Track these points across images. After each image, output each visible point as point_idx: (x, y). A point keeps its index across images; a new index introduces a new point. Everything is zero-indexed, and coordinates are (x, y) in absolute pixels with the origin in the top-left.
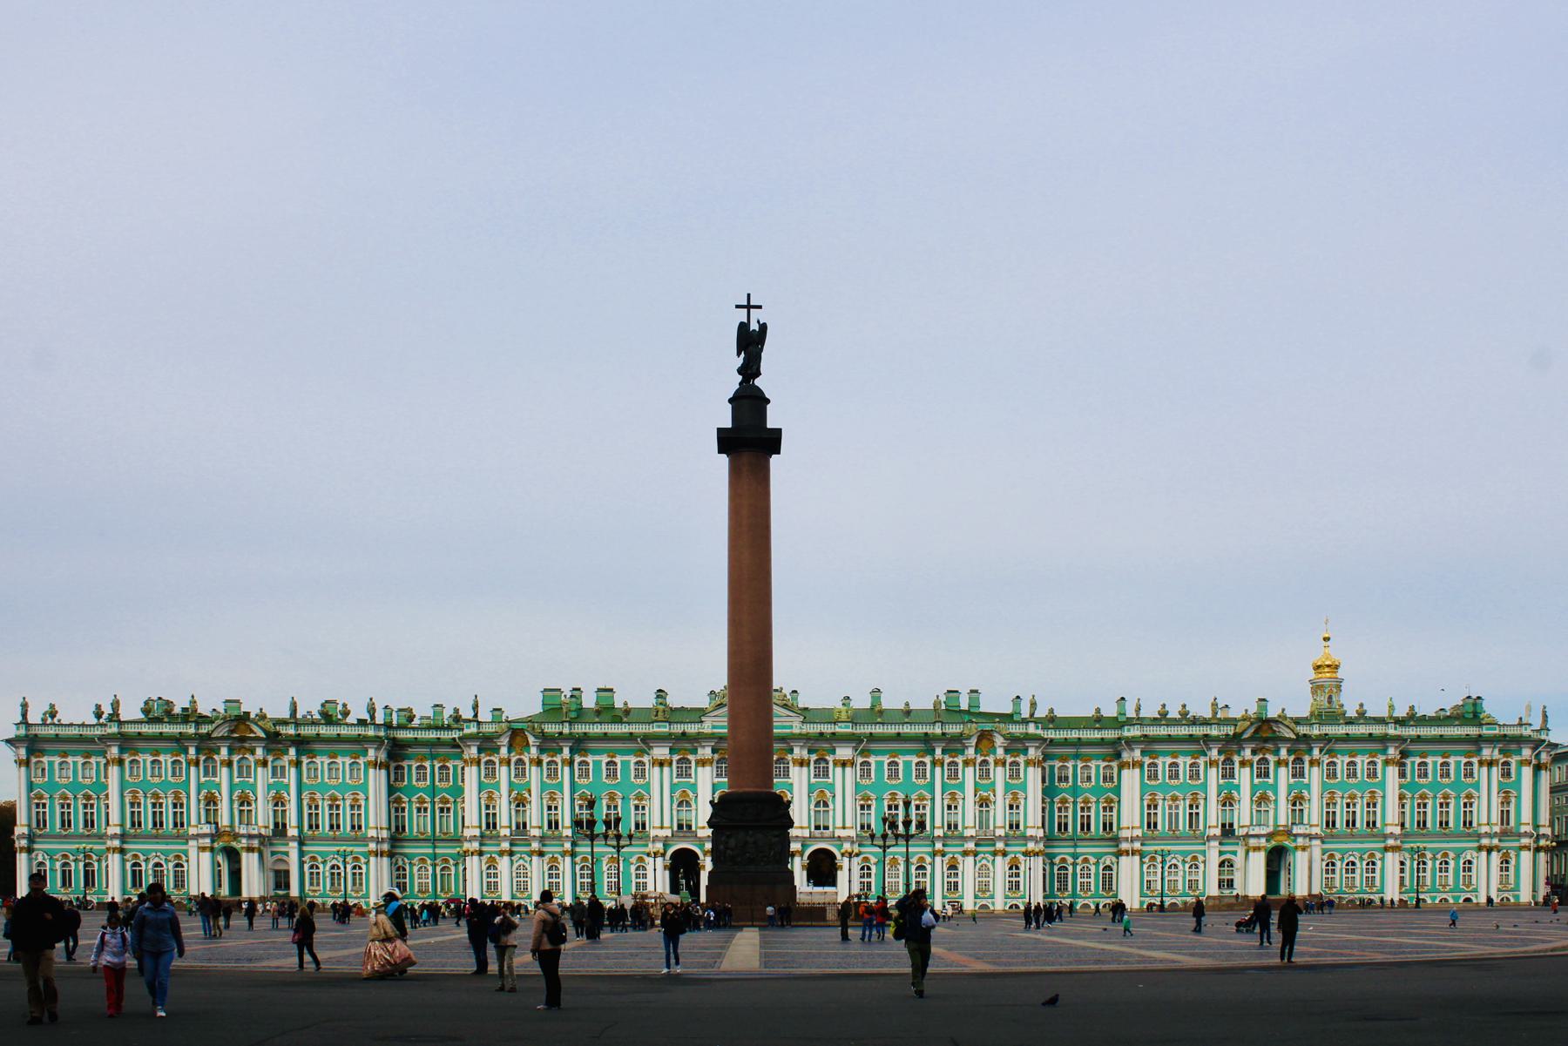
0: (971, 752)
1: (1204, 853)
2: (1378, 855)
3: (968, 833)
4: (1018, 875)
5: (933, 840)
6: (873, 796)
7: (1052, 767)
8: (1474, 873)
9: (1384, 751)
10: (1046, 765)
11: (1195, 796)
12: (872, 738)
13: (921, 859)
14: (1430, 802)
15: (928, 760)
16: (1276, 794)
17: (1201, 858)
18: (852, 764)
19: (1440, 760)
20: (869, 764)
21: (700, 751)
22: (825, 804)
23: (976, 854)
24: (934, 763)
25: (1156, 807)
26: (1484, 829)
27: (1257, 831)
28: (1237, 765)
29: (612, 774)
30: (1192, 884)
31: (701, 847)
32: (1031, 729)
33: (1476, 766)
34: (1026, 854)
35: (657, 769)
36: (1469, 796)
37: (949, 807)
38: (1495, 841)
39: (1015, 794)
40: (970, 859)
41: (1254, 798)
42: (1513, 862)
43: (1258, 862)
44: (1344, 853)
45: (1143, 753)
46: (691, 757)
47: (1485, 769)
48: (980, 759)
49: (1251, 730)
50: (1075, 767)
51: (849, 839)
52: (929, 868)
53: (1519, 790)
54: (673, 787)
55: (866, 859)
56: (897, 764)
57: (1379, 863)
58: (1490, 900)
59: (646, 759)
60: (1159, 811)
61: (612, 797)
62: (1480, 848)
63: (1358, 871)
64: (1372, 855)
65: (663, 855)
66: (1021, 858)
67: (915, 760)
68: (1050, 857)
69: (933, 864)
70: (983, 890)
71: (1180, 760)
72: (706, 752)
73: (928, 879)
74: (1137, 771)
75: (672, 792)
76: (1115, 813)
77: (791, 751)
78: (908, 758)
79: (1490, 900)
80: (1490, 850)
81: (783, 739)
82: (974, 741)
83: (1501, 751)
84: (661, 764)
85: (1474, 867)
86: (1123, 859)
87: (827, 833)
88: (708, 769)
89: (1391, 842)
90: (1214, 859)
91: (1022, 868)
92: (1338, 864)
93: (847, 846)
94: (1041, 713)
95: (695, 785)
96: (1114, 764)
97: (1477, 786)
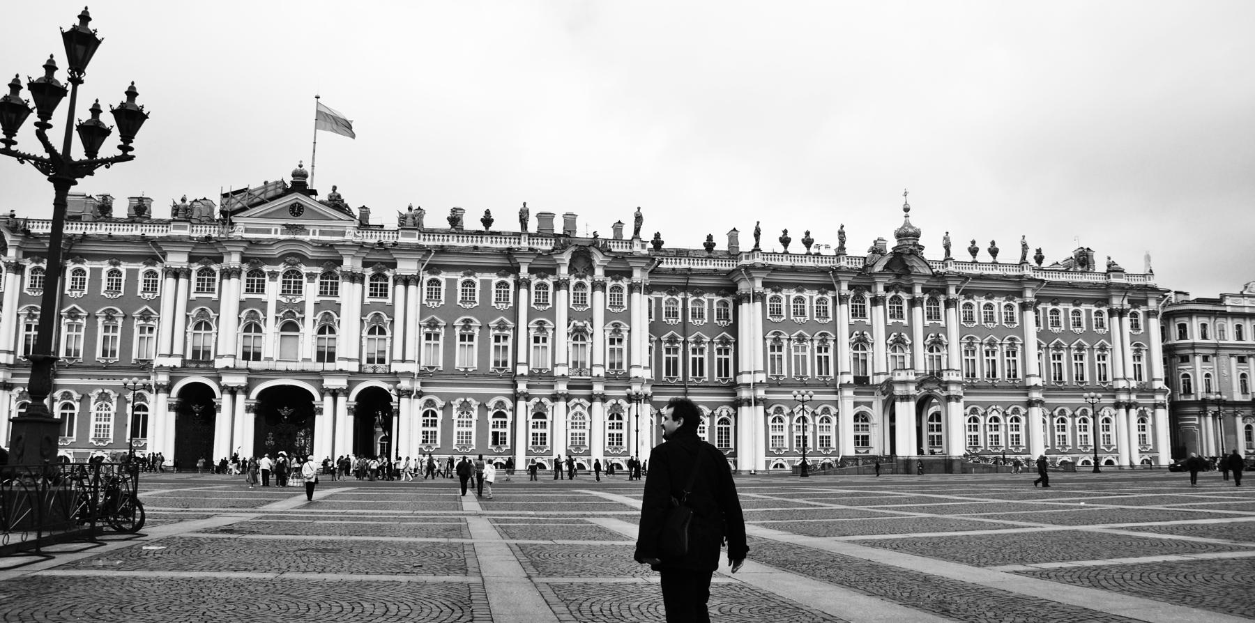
0: (563, 271)
1: (836, 403)
2: (1023, 411)
3: (559, 371)
4: (620, 426)
5: (513, 380)
6: (442, 323)
7: (659, 300)
8: (1112, 432)
9: (1020, 294)
10: (656, 295)
11: (824, 340)
12: (442, 250)
13: (501, 404)
14: (1064, 354)
15: (510, 280)
16: (911, 337)
17: (833, 410)
18: (416, 280)
19: (1071, 308)
20: (438, 283)
21: (226, 259)
22: (382, 332)
23: (568, 398)
24: (518, 285)
25: (780, 349)
26: (1122, 384)
27: (902, 376)
28: (868, 303)
29: (114, 287)
30: (825, 441)
31: (218, 379)
32: (637, 248)
33: (1106, 316)
34: (629, 399)
35: (170, 281)
36: (1103, 348)
37: (537, 340)
38: (1133, 398)
39: (616, 325)
40: (562, 405)
41: (879, 341)
42: (1150, 421)
43: (906, 413)
44: (987, 405)
45: (765, 285)
46: (214, 267)
47: (1116, 319)
48: (574, 281)
49: (884, 262)
50: (685, 301)
51: (408, 373)
52: (509, 414)
53: (1149, 344)
54: (190, 304)
55: (430, 403)
56: (473, 284)
57: (1023, 419)
58: (1132, 465)
59: (158, 268)
60: (784, 353)
61: (110, 316)
62: (1117, 406)
63: (1002, 428)
64: (1016, 411)
65: (168, 389)
66: (625, 404)
67: (495, 279)
68: (657, 406)
69: (514, 410)
70: (578, 444)
71: (806, 294)
72: (234, 260)
73: (508, 430)
74: (758, 304)
75: (189, 309)
76: (731, 357)
77: (340, 263)
78: (486, 276)
79: (1132, 465)
80: (1129, 406)
81: (331, 246)
82: (566, 257)
83: (1129, 302)
84: (176, 274)
85: (1112, 426)
86: (744, 411)
87: (381, 368)
88: (234, 280)
89: (1036, 395)
90: (848, 410)
91: (625, 417)
92: (981, 419)
93: (405, 384)
94: (647, 234)
95: (218, 302)
96: (729, 299)
97: (1108, 337)
